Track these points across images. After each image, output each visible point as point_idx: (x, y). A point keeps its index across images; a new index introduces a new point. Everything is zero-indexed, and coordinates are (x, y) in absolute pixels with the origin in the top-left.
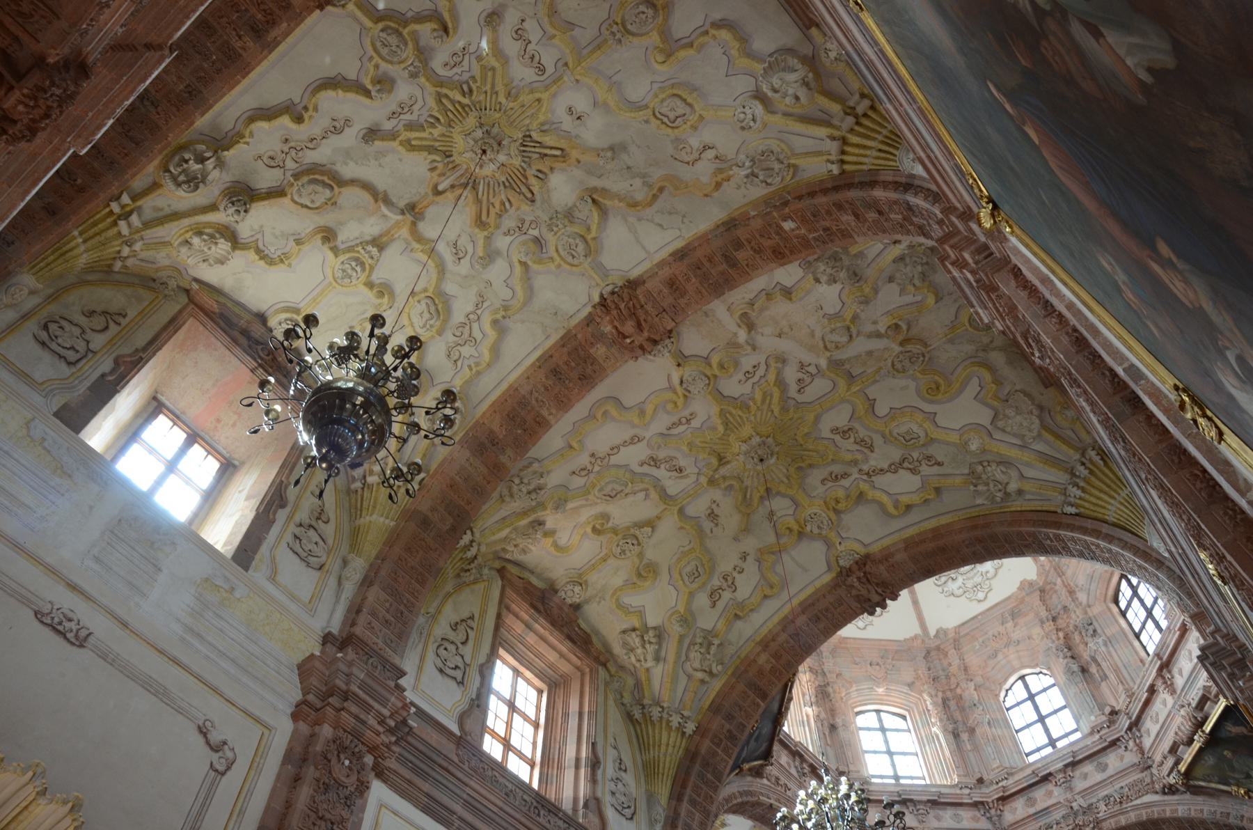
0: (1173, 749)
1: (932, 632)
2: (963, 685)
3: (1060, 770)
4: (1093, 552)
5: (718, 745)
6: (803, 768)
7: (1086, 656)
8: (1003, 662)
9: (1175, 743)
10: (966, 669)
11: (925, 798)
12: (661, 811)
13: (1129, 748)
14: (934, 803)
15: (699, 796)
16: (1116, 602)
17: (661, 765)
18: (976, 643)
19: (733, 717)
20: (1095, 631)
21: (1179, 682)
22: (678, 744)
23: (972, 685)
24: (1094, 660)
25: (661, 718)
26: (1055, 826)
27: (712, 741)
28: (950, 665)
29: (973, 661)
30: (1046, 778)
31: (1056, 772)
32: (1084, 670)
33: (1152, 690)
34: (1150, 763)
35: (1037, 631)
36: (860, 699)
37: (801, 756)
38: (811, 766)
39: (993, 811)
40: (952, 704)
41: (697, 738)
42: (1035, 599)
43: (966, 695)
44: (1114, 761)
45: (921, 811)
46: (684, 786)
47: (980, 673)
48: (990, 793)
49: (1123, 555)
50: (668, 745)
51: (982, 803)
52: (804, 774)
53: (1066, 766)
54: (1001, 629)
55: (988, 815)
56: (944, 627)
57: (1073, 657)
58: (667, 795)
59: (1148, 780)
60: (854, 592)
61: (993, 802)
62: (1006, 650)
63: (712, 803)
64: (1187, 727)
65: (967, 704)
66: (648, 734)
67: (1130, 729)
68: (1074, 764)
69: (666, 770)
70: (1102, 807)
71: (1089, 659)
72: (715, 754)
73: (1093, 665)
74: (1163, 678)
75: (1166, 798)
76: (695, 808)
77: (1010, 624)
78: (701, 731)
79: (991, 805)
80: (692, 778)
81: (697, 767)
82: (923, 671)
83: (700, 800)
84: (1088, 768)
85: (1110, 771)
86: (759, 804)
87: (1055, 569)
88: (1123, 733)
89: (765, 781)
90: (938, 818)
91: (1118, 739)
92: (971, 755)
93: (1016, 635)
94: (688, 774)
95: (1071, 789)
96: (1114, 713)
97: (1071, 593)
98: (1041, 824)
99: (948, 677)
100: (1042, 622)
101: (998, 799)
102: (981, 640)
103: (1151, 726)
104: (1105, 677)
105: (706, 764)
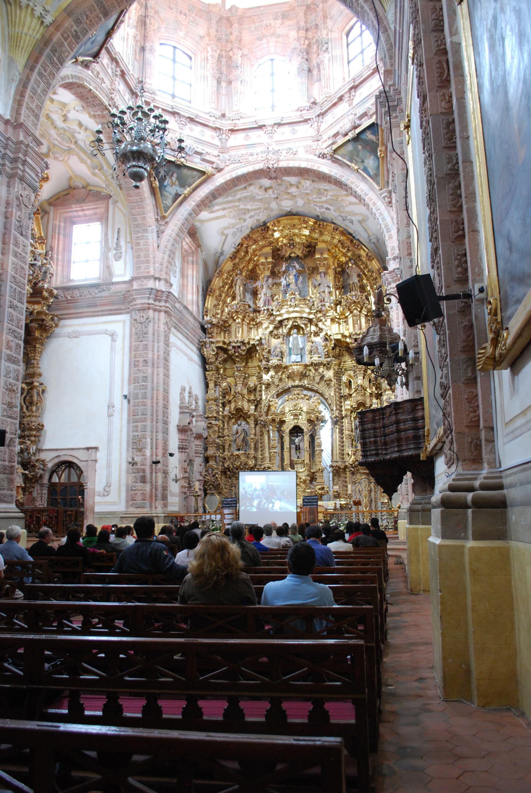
0: (336, 135)
1: (228, 7)
2: (235, 51)
4: (353, 3)
5: (66, 39)
6: (116, 71)
7: (314, 63)
9: (338, 132)
10: (240, 41)
11: (187, 115)
12: (17, 74)
13: (313, 126)
14: (191, 120)
15: (45, 71)
16: (347, 35)
17: (22, 41)
18: (253, 25)
19: (81, 22)
20: (327, 49)
21: (357, 100)
22: (37, 29)
23: (240, 53)
24: (318, 66)
25: (28, 5)
26: (255, 156)
27: (62, 35)
28: (231, 34)
29: (247, 37)
30: (261, 127)
32: (310, 71)
33: (341, 99)
34: (320, 138)
35: (293, 34)
37: (117, 62)
38: (122, 72)
39: (224, 136)
40: (224, 60)
41: (52, 29)
43: (234, 58)
45: (182, 122)
46: (36, 61)
47: (248, 46)
48: (226, 125)
49: (368, 14)
50: (29, 27)
51: (220, 129)
52: (116, 75)
53: (275, 124)
54: (272, 22)
55: (220, 137)
56: (237, 6)
57: (307, 60)
58: (24, 64)
59: (314, 147)
62: (269, 38)
63: (54, 78)
64: (348, 126)
65: (233, 64)
66: (16, 14)
67: (318, 116)
68: (279, 125)
69: (25, 46)
70: (284, 152)
71: (315, 64)
72: (62, 45)
73: (316, 70)
75: (320, 159)
76: (41, 79)
77: (279, 22)
78: (56, 25)
80: (43, 58)
81: (48, 51)
82: (213, 32)
83: (46, 74)
84: (286, 129)
85: (297, 136)
86: (83, 86)
88: (314, 117)
89: (90, 72)
90: (191, 130)
91: (309, 119)
92: (223, 97)
93: (280, 31)
94: (41, 53)
95: (272, 137)
96: (314, 103)
97: (325, 17)
98: (248, 152)
99: (227, 41)
100: (299, 29)
101: (229, 130)
102: (257, 24)
103: (329, 118)
104: (319, 80)
105: (54, 51)
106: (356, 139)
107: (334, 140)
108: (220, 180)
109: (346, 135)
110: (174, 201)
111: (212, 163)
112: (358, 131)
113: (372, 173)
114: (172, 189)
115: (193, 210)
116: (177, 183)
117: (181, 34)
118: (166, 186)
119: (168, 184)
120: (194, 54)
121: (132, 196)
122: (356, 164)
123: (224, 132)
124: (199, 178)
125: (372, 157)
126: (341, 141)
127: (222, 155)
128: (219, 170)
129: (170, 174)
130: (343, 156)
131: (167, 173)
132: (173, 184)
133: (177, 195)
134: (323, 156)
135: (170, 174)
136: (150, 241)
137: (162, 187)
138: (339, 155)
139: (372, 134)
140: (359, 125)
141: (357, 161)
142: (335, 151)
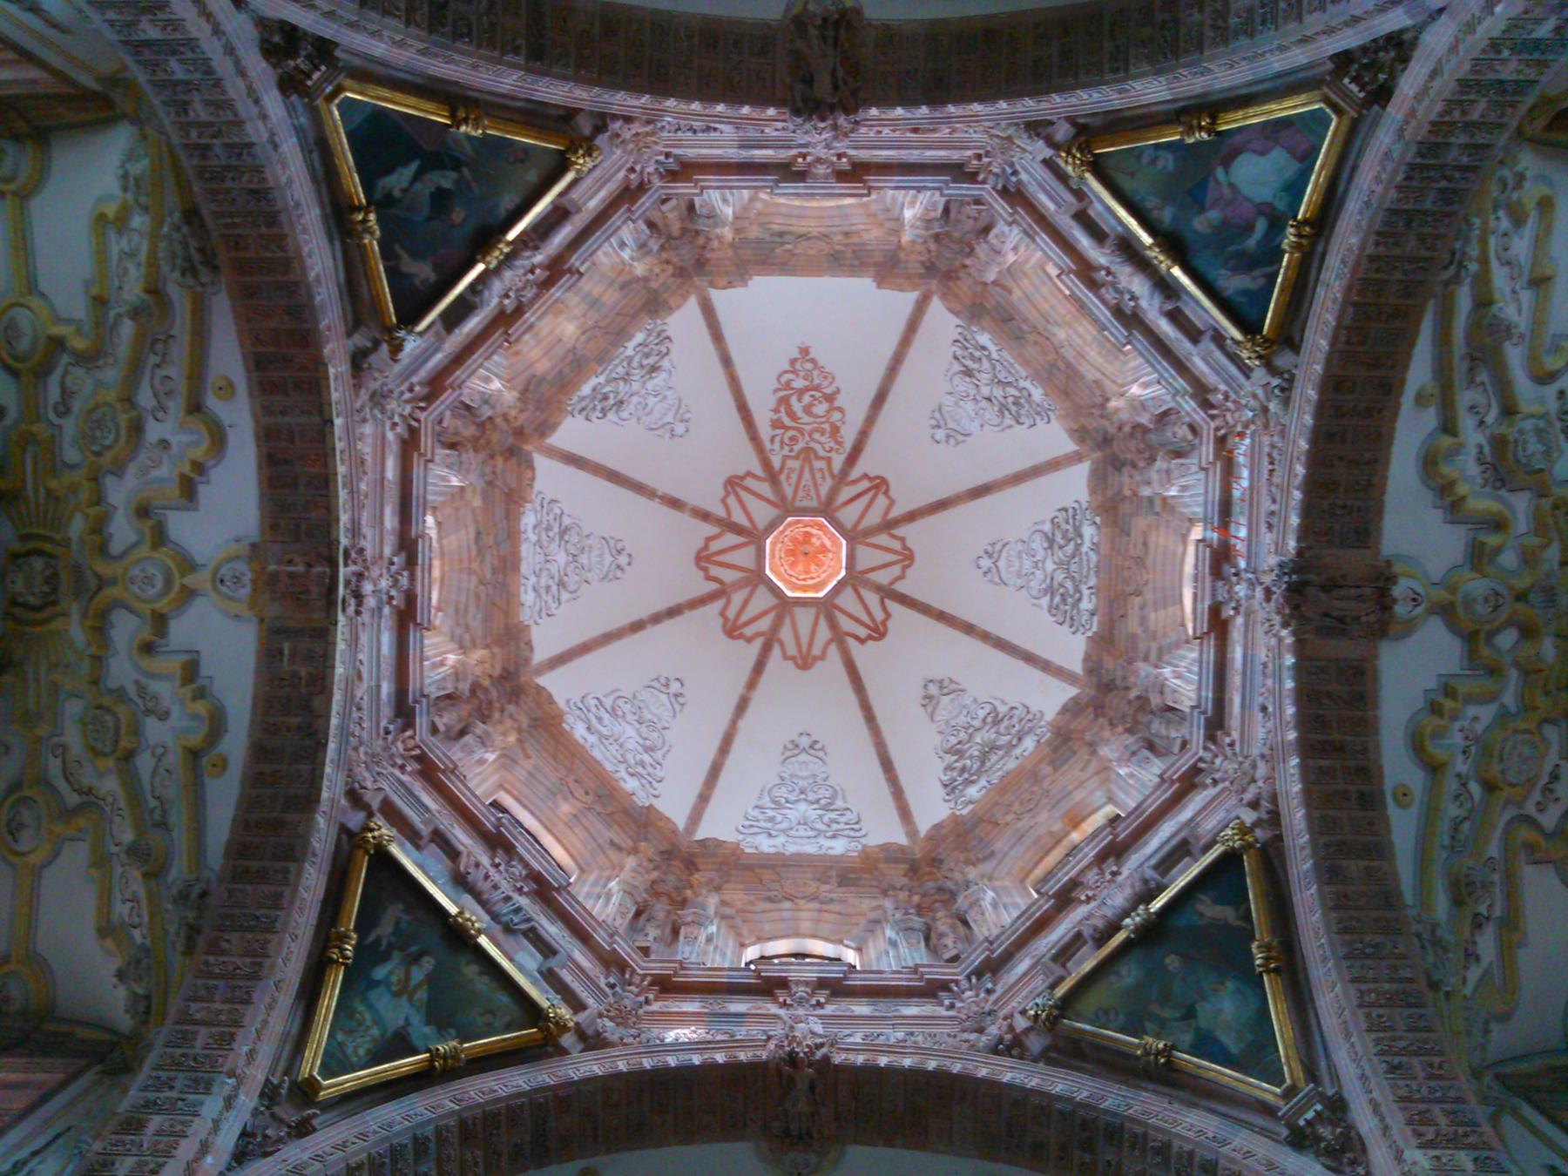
0: (1064, 954)
1: (700, 835)
3: (807, 983)
8: (787, 914)
11: (536, 866)
31: (798, 983)
36: (524, 789)
37: (411, 563)
39: (632, 988)
42: (897, 875)
44: (912, 1010)
60: (800, 44)
61: (645, 976)
67: (979, 973)
74: (1102, 873)
79: (637, 979)
87: (958, 836)
91: (944, 986)
106: (1153, 934)
107: (1058, 971)
108: (583, 1066)
109: (1114, 927)
110: (376, 1059)
111: (577, 1005)
112: (1157, 905)
113: (1234, 1048)
114: (393, 1011)
115: (438, 1131)
116: (422, 995)
117: (566, 808)
118: (377, 984)
119: (386, 982)
120: (582, 870)
121: (224, 952)
122: (1158, 1036)
123: (637, 979)
124: (508, 1029)
125: (1230, 985)
126: (1087, 962)
127: (609, 1024)
128: (593, 1041)
129: (414, 949)
130: (1101, 1018)
131: (402, 941)
132: (403, 990)
133: (399, 1044)
134: (1011, 1047)
135: (414, 949)
136: (200, 1128)
137: (357, 981)
138: (1080, 1018)
139: (1218, 901)
140: (1161, 889)
141: (1163, 1023)
142: (1066, 1005)
